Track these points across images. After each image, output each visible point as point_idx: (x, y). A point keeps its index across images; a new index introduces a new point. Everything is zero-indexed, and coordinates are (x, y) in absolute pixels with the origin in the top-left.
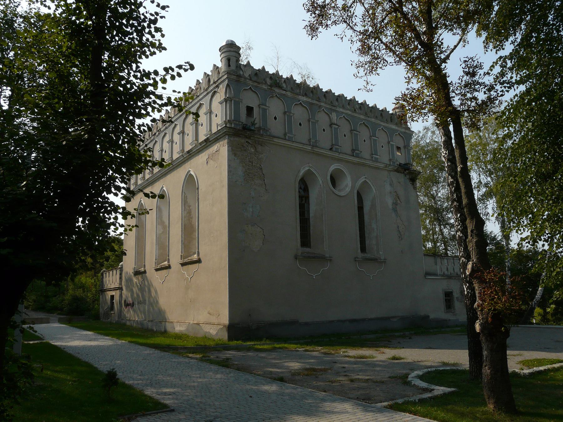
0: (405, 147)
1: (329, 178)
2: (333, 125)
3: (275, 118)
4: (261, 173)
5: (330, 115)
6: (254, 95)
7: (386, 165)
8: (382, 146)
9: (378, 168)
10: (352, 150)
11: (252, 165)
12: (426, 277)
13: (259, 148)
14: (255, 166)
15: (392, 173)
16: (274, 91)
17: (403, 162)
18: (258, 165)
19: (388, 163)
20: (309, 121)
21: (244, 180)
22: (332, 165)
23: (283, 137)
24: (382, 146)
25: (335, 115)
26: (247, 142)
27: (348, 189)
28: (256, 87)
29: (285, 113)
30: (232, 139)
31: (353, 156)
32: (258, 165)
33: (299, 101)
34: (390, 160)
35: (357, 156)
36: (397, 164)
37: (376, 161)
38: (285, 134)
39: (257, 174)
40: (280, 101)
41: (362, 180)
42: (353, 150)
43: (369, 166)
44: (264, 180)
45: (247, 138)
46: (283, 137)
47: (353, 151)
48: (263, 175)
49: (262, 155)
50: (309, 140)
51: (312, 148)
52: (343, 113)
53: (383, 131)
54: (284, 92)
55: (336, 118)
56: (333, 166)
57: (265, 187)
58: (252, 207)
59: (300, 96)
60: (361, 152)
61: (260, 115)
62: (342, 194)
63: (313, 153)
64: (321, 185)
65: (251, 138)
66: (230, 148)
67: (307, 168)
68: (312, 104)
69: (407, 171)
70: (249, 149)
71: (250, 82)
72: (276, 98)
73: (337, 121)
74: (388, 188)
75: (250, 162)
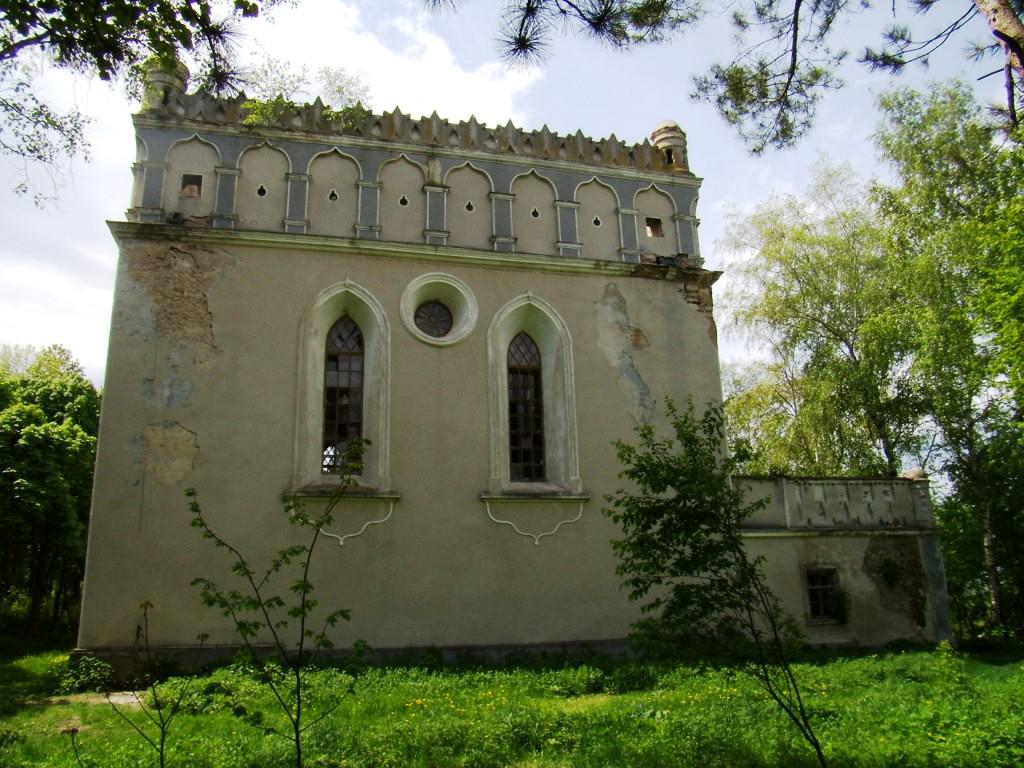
3: (262, 192)
5: (425, 168)
6: (206, 151)
7: (594, 262)
9: (574, 273)
11: (182, 297)
13: (203, 257)
14: (188, 297)
16: (259, 135)
22: (414, 277)
26: (172, 248)
28: (210, 133)
30: (128, 246)
33: (331, 147)
40: (276, 154)
43: (544, 270)
44: (211, 326)
45: (171, 240)
49: (212, 273)
51: (351, 243)
52: (463, 158)
53: (599, 188)
54: (287, 133)
56: (420, 277)
59: (331, 137)
63: (360, 254)
65: (183, 239)
66: (126, 265)
68: (365, 149)
70: (179, 262)
71: (195, 126)
72: (265, 150)
75: (176, 290)
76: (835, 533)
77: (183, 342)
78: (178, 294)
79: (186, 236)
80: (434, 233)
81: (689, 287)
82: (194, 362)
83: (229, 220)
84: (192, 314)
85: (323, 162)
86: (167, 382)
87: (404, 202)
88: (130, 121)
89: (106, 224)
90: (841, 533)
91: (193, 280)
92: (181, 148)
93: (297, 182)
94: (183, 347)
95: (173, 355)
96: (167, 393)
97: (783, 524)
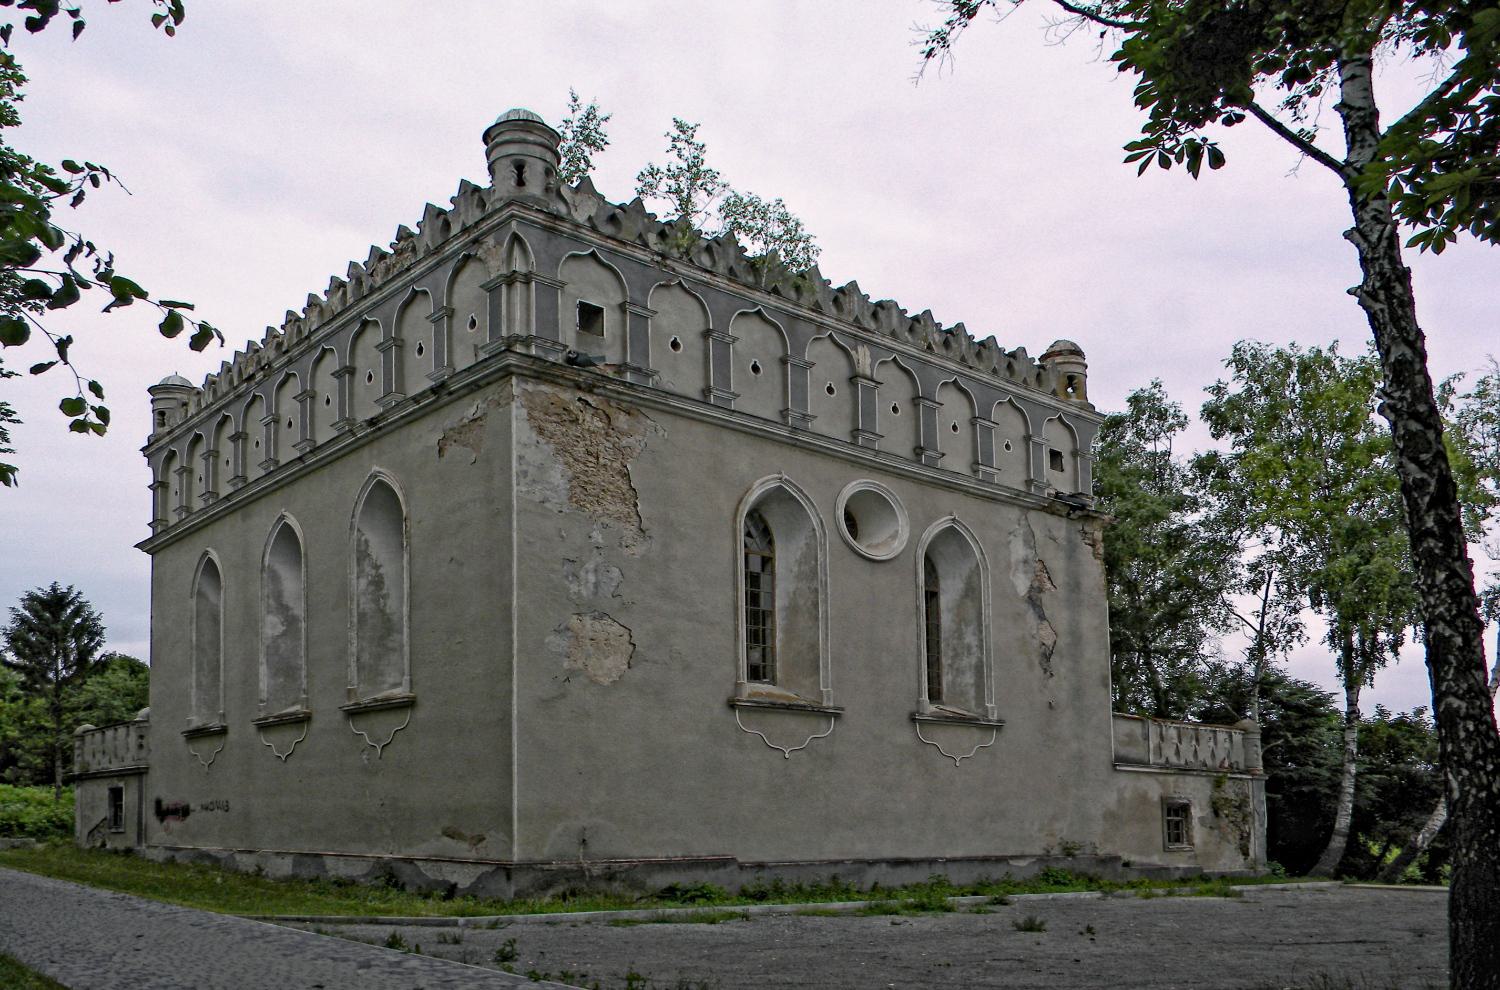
0: (1075, 454)
1: (841, 513)
2: (860, 379)
4: (625, 487)
8: (1008, 447)
10: (914, 450)
15: (1032, 515)
17: (1067, 490)
18: (615, 465)
19: (1022, 488)
20: (783, 361)
21: (570, 498)
23: (697, 396)
24: (1008, 447)
25: (868, 353)
27: (898, 546)
29: (706, 334)
31: (919, 461)
32: (617, 465)
34: (1029, 482)
35: (931, 465)
36: (1049, 494)
37: (988, 480)
38: (706, 391)
39: (611, 487)
41: (942, 523)
42: (918, 450)
44: (636, 505)
46: (697, 396)
47: (918, 451)
48: (631, 492)
49: (631, 440)
50: (784, 413)
55: (868, 361)
56: (854, 483)
57: (636, 524)
58: (596, 571)
60: (943, 455)
61: (625, 332)
62: (881, 554)
64: (814, 530)
67: (773, 485)
69: (1079, 513)
73: (872, 370)
74: (1019, 550)
77: (605, 520)
78: (591, 459)
79: (604, 387)
83: (648, 375)
84: (611, 487)
85: (743, 321)
86: (590, 566)
91: (608, 444)
94: (605, 526)
95: (594, 534)
96: (592, 578)
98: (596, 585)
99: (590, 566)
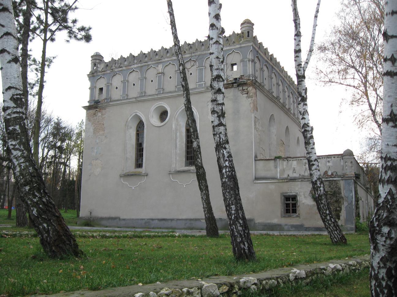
12: (254, 182)
13: (104, 111)
28: (104, 74)
51: (136, 99)
76: (297, 180)
80: (161, 89)
81: (244, 88)
82: (101, 141)
86: (96, 148)
87: (152, 81)
88: (87, 76)
89: (82, 108)
90: (300, 180)
92: (99, 80)
93: (125, 82)
96: (96, 151)
97: (276, 177)
98: (97, 152)
99: (96, 148)
